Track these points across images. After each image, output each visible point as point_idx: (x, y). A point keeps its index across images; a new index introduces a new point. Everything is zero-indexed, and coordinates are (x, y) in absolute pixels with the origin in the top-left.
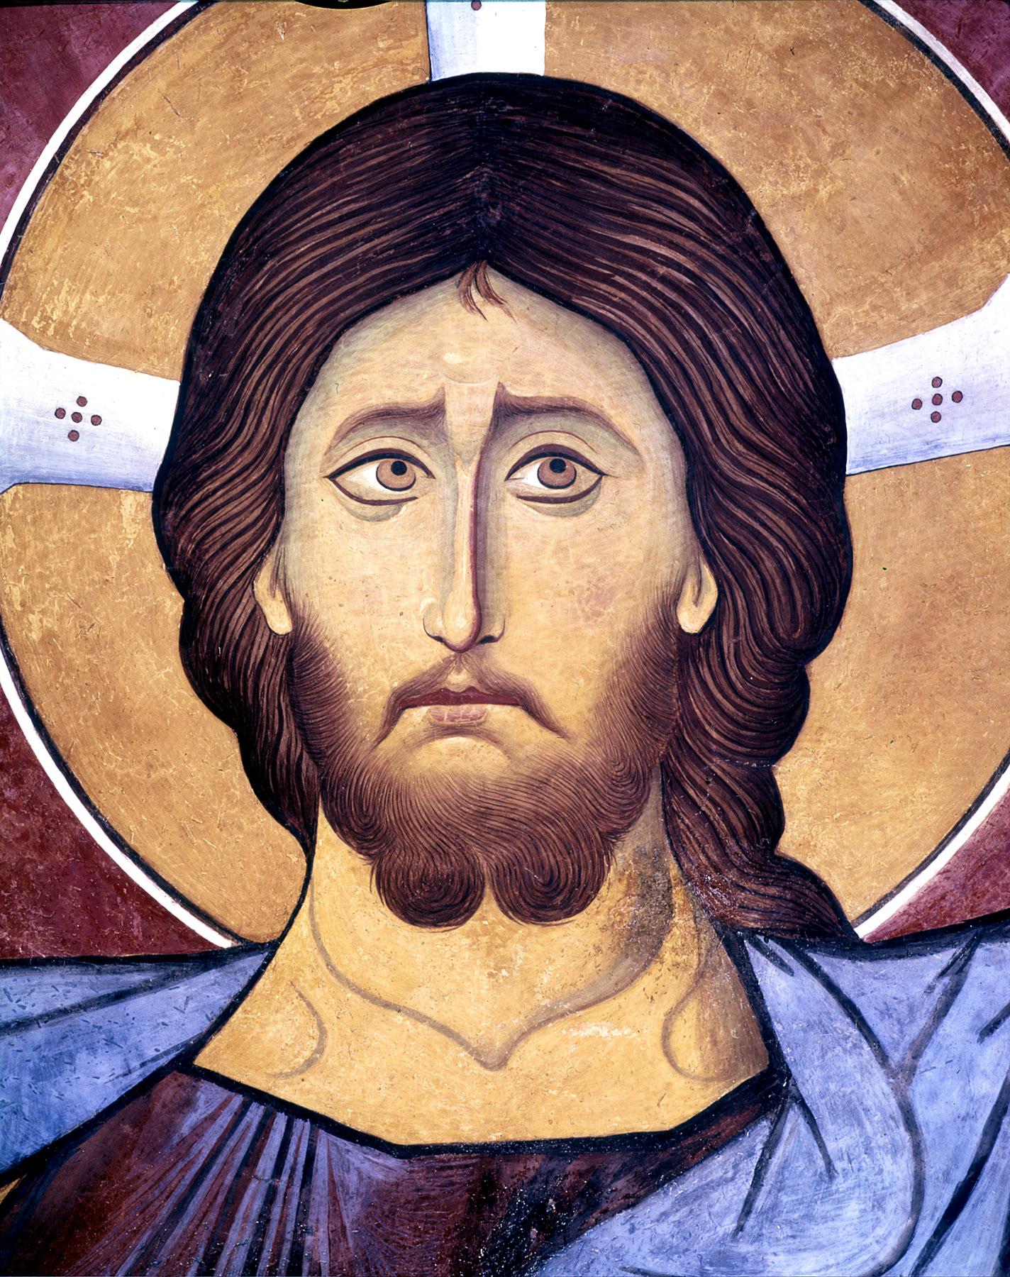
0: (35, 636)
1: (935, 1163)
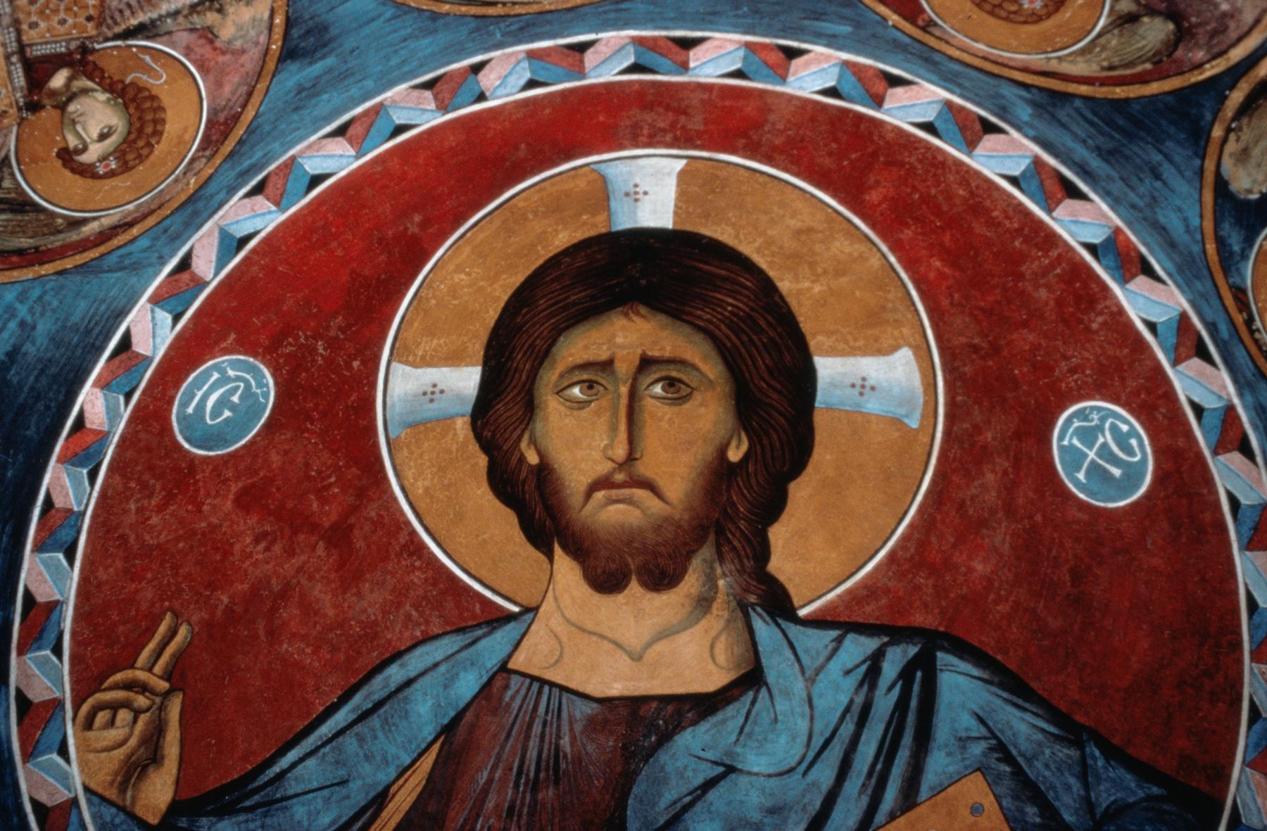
0: (420, 491)
1: (818, 726)
